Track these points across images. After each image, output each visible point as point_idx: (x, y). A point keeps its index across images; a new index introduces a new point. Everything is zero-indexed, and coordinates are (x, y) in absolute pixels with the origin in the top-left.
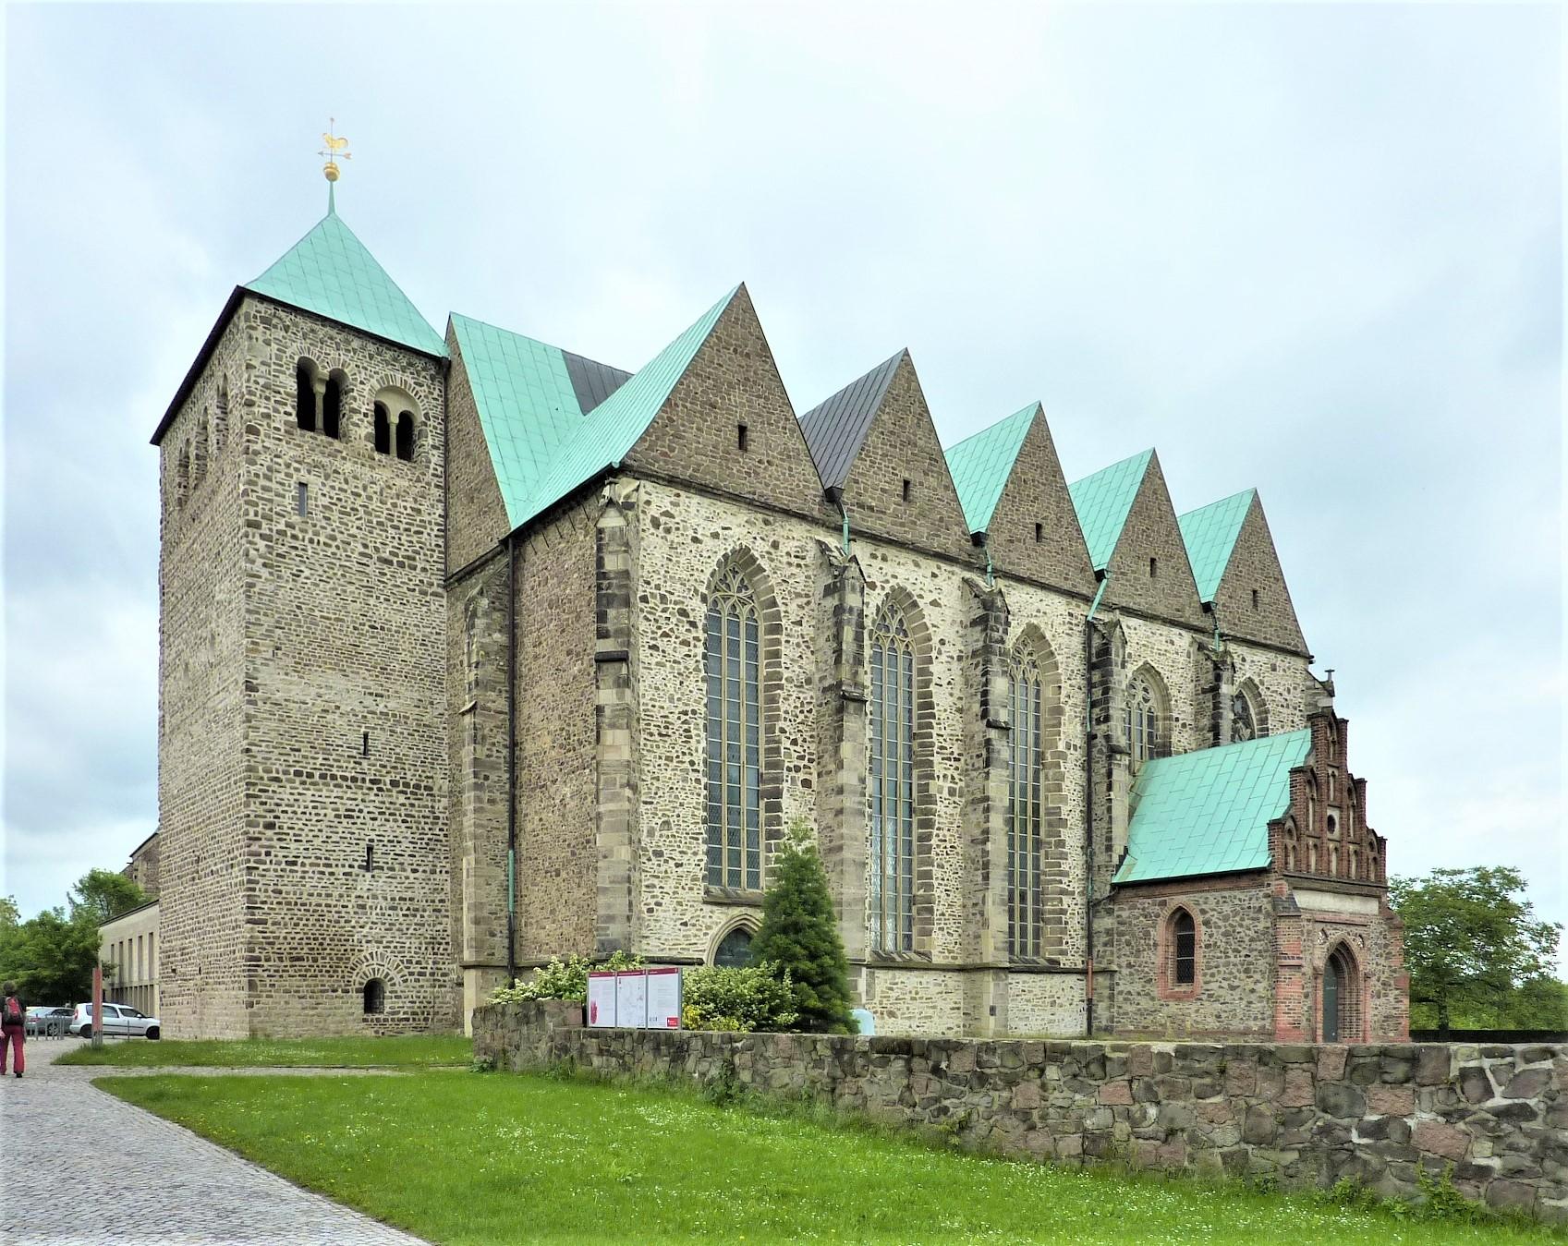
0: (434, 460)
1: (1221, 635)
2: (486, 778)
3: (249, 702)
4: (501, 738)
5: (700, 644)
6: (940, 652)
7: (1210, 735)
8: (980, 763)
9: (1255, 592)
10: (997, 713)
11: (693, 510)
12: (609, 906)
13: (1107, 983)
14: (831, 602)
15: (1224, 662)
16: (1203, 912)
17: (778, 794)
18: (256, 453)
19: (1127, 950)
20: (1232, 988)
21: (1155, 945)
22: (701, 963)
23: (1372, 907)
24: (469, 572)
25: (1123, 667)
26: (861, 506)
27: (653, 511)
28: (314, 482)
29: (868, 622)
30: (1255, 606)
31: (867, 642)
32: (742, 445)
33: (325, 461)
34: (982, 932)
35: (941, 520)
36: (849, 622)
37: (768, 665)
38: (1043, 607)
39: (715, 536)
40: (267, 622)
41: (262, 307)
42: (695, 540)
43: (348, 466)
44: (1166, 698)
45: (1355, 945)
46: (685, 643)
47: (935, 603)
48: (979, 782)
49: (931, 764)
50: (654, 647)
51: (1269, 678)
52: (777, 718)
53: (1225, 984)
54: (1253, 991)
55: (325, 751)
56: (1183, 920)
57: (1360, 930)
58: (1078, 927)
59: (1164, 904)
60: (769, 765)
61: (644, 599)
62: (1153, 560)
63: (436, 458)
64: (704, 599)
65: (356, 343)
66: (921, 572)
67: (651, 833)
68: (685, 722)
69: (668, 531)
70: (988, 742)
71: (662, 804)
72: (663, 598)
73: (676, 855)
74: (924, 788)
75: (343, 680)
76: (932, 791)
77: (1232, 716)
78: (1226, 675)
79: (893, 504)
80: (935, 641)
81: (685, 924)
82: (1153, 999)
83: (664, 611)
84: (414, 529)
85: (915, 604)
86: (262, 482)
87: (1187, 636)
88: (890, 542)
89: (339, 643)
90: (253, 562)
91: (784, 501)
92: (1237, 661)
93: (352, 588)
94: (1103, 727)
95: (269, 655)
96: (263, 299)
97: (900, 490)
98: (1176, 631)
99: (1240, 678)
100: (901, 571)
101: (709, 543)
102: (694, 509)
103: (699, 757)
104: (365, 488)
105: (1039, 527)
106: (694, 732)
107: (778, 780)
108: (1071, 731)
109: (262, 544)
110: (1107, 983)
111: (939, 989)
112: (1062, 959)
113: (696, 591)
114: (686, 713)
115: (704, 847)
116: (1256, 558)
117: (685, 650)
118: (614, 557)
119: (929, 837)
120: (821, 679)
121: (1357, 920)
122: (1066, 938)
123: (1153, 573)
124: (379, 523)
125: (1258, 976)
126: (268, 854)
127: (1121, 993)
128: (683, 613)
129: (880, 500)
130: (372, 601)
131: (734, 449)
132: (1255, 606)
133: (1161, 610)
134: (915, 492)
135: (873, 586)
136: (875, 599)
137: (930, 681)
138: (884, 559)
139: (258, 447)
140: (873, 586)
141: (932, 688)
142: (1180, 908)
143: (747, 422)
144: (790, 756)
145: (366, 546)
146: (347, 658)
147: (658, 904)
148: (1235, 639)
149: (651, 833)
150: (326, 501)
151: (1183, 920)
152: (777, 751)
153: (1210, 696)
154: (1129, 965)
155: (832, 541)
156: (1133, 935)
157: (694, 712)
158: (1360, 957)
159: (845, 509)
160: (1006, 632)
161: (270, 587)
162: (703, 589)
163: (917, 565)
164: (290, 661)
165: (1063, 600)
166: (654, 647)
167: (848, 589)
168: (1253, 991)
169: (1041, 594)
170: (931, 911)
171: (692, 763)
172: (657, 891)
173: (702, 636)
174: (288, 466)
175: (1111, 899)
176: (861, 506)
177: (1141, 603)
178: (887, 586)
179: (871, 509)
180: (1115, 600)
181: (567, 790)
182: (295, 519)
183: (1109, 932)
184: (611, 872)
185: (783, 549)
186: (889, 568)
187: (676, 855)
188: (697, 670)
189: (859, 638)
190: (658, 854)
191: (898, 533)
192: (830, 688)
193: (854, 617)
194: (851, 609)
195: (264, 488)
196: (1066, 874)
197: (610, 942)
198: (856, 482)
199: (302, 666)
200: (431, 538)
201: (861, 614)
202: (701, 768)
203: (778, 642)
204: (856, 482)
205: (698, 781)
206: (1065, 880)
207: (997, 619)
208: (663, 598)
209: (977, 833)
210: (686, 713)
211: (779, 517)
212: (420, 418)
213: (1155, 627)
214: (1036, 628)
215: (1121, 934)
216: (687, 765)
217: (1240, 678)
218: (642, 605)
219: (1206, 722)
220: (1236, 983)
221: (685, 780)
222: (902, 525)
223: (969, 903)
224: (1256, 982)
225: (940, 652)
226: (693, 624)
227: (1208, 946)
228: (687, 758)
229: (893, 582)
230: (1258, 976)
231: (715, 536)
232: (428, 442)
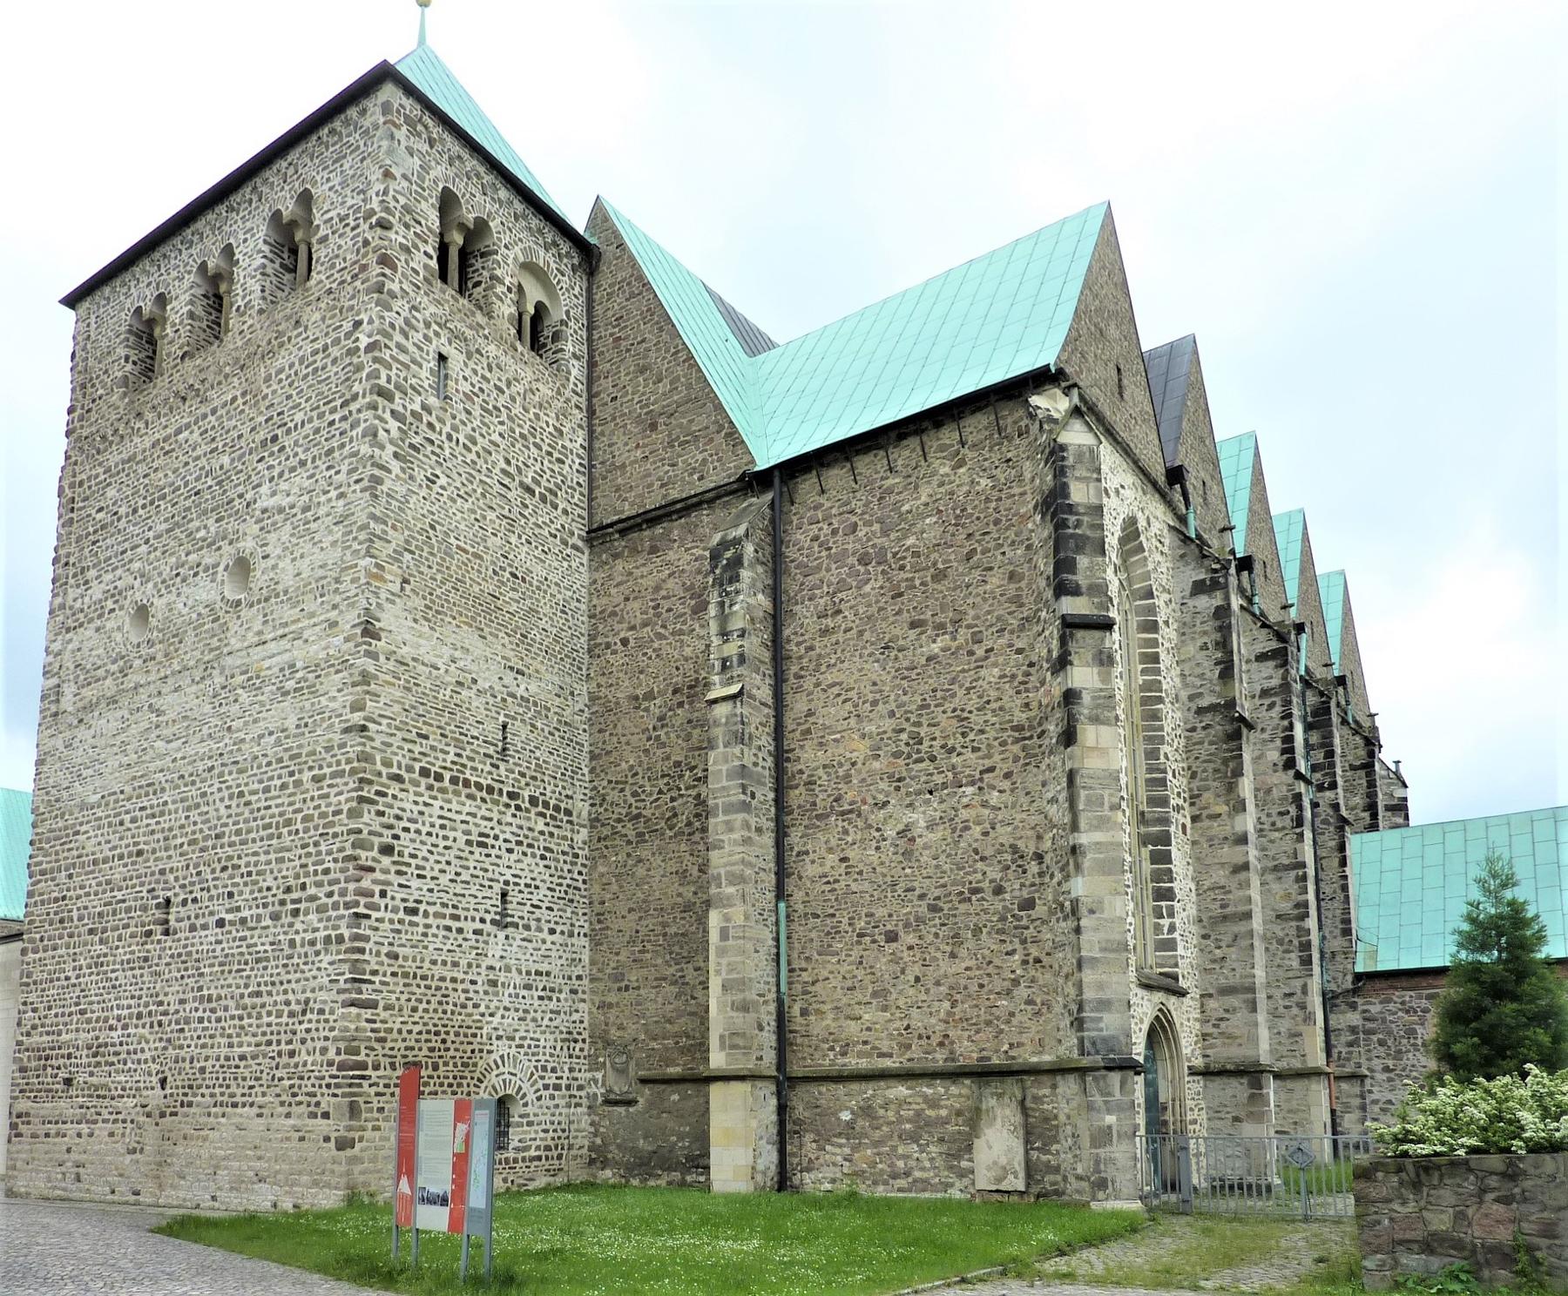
0: (574, 372)
2: (753, 796)
3: (368, 654)
4: (766, 740)
8: (1287, 821)
12: (1101, 986)
13: (1357, 1090)
14: (1206, 603)
17: (1165, 839)
18: (393, 295)
19: (1381, 1051)
24: (629, 526)
28: (456, 359)
33: (469, 333)
34: (1302, 1028)
37: (1144, 672)
40: (397, 538)
41: (408, 103)
43: (492, 347)
48: (1287, 844)
52: (1161, 740)
55: (458, 744)
60: (1152, 801)
63: (576, 370)
65: (503, 194)
75: (480, 643)
84: (556, 455)
86: (398, 337)
89: (476, 588)
90: (382, 448)
93: (491, 515)
94: (1329, 794)
95: (396, 588)
96: (410, 90)
104: (509, 384)
107: (1165, 821)
109: (393, 425)
110: (1357, 1090)
120: (1191, 698)
124: (522, 436)
126: (383, 894)
127: (1375, 1102)
130: (513, 539)
139: (395, 287)
145: (508, 462)
146: (485, 613)
150: (466, 387)
152: (1163, 783)
154: (1387, 1069)
156: (1390, 1033)
161: (401, 489)
164: (418, 602)
174: (428, 325)
175: (1355, 991)
181: (918, 818)
182: (433, 401)
183: (1353, 1030)
184: (1101, 935)
192: (1213, 708)
195: (399, 346)
197: (1104, 1040)
199: (432, 613)
200: (572, 470)
203: (1155, 643)
209: (1286, 907)
212: (556, 314)
215: (1369, 1032)
223: (1278, 994)
232: (572, 345)
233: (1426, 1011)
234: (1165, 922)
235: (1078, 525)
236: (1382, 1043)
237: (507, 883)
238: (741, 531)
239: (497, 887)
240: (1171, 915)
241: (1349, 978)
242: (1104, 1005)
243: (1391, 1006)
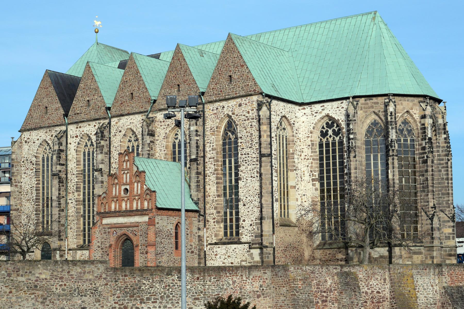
11: (34, 135)
26: (75, 114)
35: (99, 107)
36: (55, 154)
38: (132, 121)
39: (38, 139)
42: (34, 142)
45: (131, 235)
46: (32, 170)
51: (237, 111)
66: (90, 127)
69: (28, 143)
100: (85, 129)
101: (37, 142)
129: (81, 110)
169: (131, 117)
179: (78, 114)
186: (81, 129)
198: (74, 108)
222: (87, 114)
229: (83, 133)
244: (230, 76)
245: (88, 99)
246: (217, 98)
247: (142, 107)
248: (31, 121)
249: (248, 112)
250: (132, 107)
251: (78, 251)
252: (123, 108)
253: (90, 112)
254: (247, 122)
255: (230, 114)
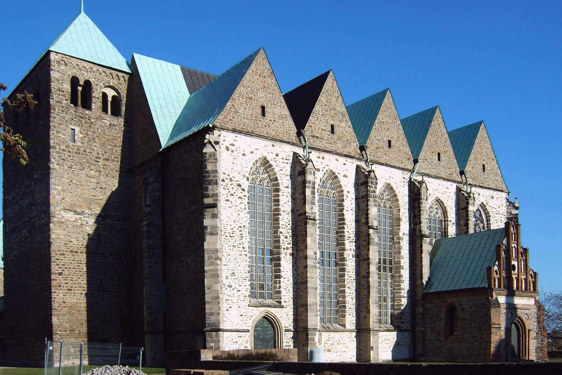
1: (470, 185)
5: (246, 198)
6: (347, 197)
7: (465, 228)
9: (484, 165)
10: (373, 223)
12: (211, 309)
14: (300, 179)
15: (470, 197)
16: (461, 305)
20: (473, 337)
21: (441, 319)
22: (248, 331)
23: (532, 302)
25: (427, 200)
26: (313, 136)
27: (227, 144)
29: (317, 186)
30: (484, 171)
31: (316, 194)
32: (263, 114)
35: (347, 140)
36: (309, 187)
37: (274, 205)
39: (252, 152)
44: (445, 212)
47: (345, 176)
49: (344, 244)
50: (228, 200)
53: (470, 335)
54: (482, 338)
56: (452, 309)
57: (527, 311)
58: (409, 311)
59: (445, 302)
61: (223, 181)
62: (439, 154)
64: (248, 179)
67: (227, 278)
68: (241, 231)
69: (232, 151)
70: (369, 235)
71: (231, 265)
72: (231, 180)
73: (237, 287)
74: (342, 254)
76: (346, 256)
77: (474, 219)
78: (471, 202)
79: (327, 135)
80: (345, 193)
81: (242, 315)
82: (441, 342)
83: (231, 185)
85: (336, 177)
87: (454, 185)
88: (326, 151)
91: (281, 137)
92: (476, 196)
94: (418, 226)
97: (330, 129)
98: (450, 183)
99: (478, 202)
102: (243, 141)
103: (246, 245)
105: (390, 142)
106: (244, 235)
107: (279, 253)
108: (405, 227)
111: (349, 340)
112: (402, 325)
113: (244, 176)
114: (241, 227)
115: (249, 283)
116: (484, 150)
117: (240, 201)
118: (211, 164)
119: (344, 275)
121: (525, 307)
122: (404, 316)
123: (439, 159)
125: (483, 332)
127: (427, 339)
128: (239, 185)
131: (260, 116)
132: (484, 171)
133: (443, 175)
134: (336, 129)
135: (318, 170)
136: (319, 175)
137: (343, 209)
138: (323, 158)
140: (318, 170)
141: (345, 212)
142: (451, 304)
143: (265, 105)
144: (284, 243)
147: (230, 307)
148: (475, 186)
149: (227, 278)
151: (452, 309)
152: (279, 241)
153: (464, 211)
154: (431, 328)
155: (300, 151)
157: (244, 226)
158: (527, 323)
159: (306, 138)
160: (376, 188)
162: (247, 175)
163: (337, 160)
165: (401, 172)
166: (228, 200)
167: (308, 173)
168: (482, 338)
170: (345, 307)
171: (244, 248)
172: (230, 302)
173: (247, 195)
176: (313, 136)
177: (434, 172)
178: (325, 170)
179: (317, 137)
180: (423, 171)
185: (280, 157)
187: (237, 287)
188: (245, 209)
189: (313, 193)
190: (230, 286)
191: (329, 147)
193: (311, 185)
194: (310, 182)
196: (404, 289)
197: (211, 323)
198: (311, 126)
201: (314, 183)
202: (247, 250)
204: (311, 126)
205: (246, 255)
206: (402, 291)
207: (372, 183)
208: (231, 180)
210: (241, 227)
211: (278, 143)
213: (441, 181)
214: (389, 184)
216: (241, 249)
217: (478, 202)
218: (222, 183)
219: (462, 222)
220: (475, 335)
221: (241, 255)
222: (331, 143)
224: (484, 334)
225: (347, 197)
226: (243, 190)
227: (463, 320)
228: (241, 246)
229: (327, 168)
230: (483, 332)
231: (252, 152)
233: (442, 306)
234: (278, 285)
235: (209, 176)
236: (430, 318)
237: (102, 279)
238: (148, 175)
239: (99, 281)
240: (280, 283)
241: (421, 295)
242: (212, 314)
243: (433, 305)
244: (484, 165)
245: (332, 122)
246: (474, 183)
247: (402, 163)
248: (234, 118)
249: (499, 207)
250: (390, 158)
251: (323, 333)
252: (379, 154)
253: (336, 142)
254: (497, 216)
255: (485, 204)
